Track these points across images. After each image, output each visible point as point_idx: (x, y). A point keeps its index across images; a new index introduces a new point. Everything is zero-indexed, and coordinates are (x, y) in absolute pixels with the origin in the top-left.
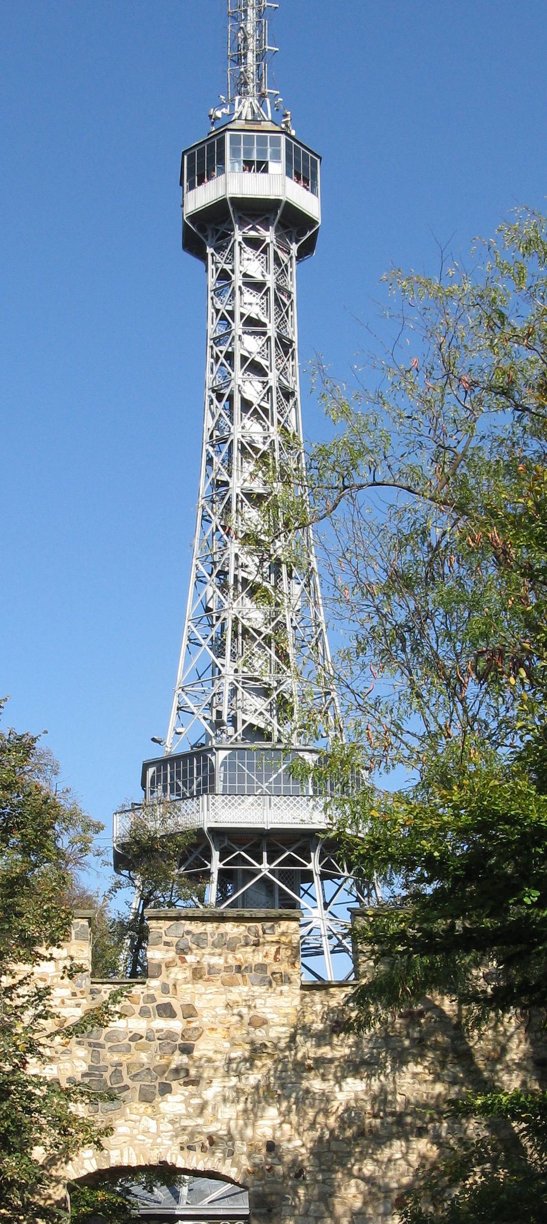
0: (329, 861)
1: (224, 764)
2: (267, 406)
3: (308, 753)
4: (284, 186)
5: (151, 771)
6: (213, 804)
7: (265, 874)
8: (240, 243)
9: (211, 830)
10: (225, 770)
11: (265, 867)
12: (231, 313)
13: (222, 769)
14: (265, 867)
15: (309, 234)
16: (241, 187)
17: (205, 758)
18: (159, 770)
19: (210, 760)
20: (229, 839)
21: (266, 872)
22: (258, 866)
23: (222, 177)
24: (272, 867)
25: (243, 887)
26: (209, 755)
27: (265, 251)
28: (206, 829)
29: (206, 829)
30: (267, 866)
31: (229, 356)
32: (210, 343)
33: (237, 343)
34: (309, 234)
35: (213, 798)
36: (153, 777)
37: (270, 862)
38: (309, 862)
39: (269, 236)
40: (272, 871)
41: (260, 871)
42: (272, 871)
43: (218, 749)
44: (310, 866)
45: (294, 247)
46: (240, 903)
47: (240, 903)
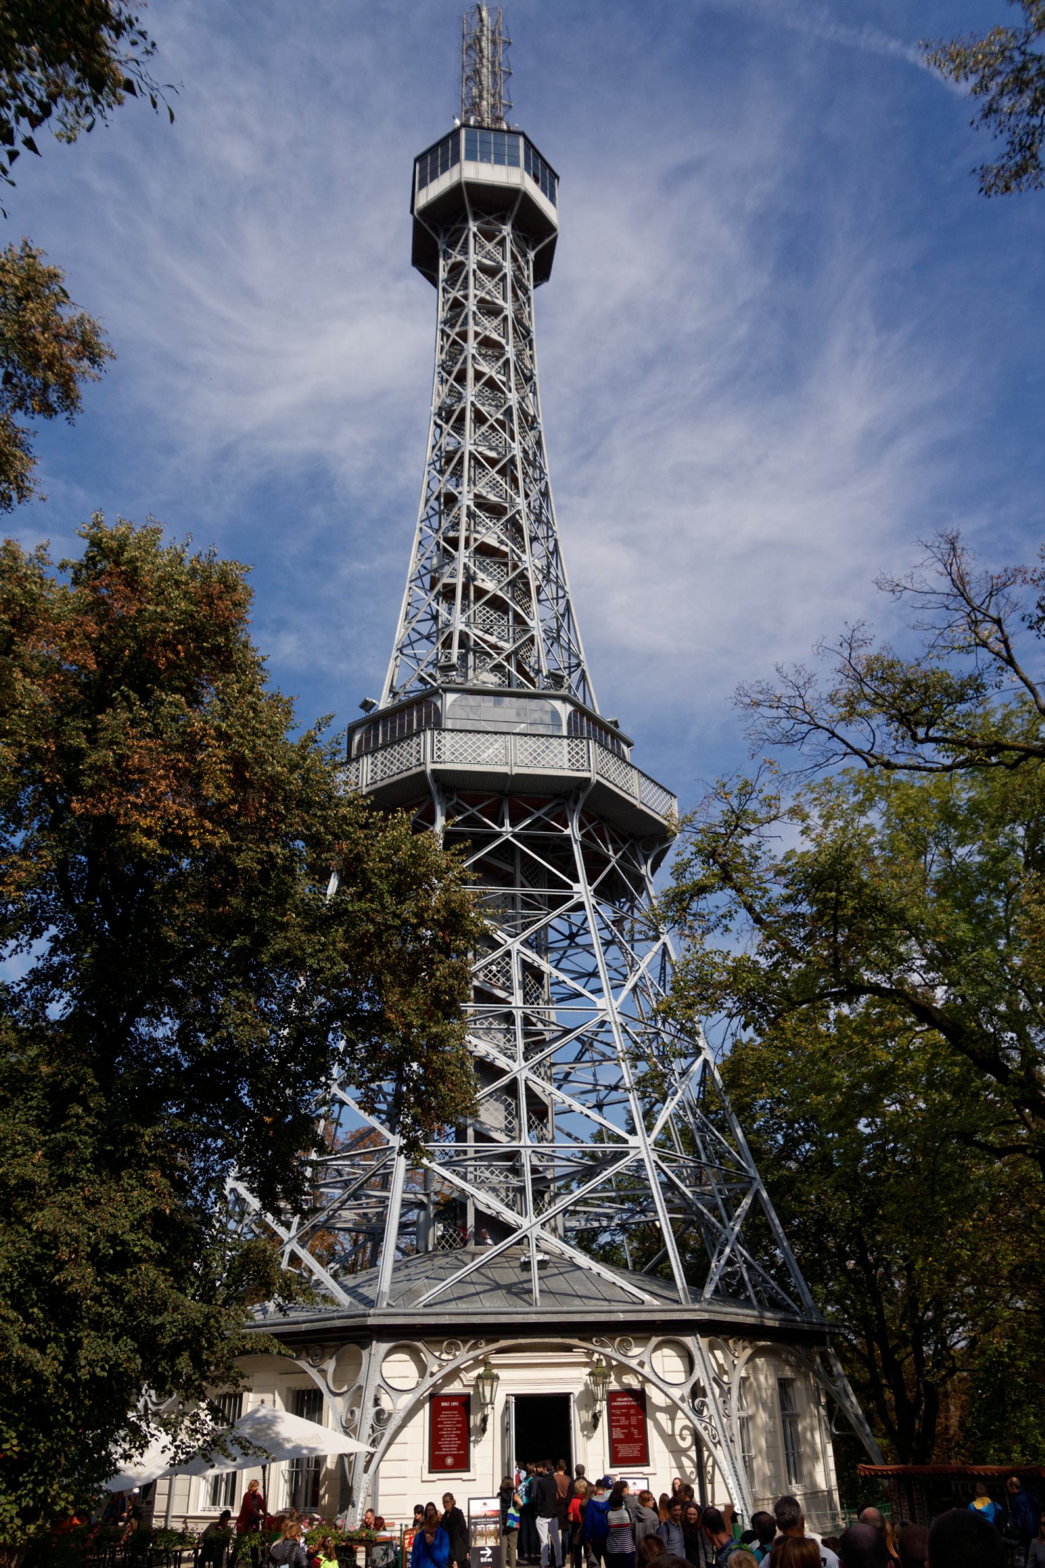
0: (588, 832)
2: (504, 379)
4: (523, 178)
7: (507, 841)
8: (475, 235)
9: (433, 771)
11: (507, 830)
12: (466, 297)
14: (507, 830)
15: (547, 240)
16: (477, 172)
18: (368, 732)
20: (459, 797)
22: (498, 829)
23: (457, 167)
27: (502, 243)
28: (428, 771)
29: (428, 771)
30: (510, 829)
31: (463, 335)
34: (547, 240)
36: (360, 742)
37: (513, 825)
38: (566, 827)
39: (507, 229)
40: (515, 836)
41: (499, 835)
43: (445, 691)
44: (567, 832)
45: (531, 255)
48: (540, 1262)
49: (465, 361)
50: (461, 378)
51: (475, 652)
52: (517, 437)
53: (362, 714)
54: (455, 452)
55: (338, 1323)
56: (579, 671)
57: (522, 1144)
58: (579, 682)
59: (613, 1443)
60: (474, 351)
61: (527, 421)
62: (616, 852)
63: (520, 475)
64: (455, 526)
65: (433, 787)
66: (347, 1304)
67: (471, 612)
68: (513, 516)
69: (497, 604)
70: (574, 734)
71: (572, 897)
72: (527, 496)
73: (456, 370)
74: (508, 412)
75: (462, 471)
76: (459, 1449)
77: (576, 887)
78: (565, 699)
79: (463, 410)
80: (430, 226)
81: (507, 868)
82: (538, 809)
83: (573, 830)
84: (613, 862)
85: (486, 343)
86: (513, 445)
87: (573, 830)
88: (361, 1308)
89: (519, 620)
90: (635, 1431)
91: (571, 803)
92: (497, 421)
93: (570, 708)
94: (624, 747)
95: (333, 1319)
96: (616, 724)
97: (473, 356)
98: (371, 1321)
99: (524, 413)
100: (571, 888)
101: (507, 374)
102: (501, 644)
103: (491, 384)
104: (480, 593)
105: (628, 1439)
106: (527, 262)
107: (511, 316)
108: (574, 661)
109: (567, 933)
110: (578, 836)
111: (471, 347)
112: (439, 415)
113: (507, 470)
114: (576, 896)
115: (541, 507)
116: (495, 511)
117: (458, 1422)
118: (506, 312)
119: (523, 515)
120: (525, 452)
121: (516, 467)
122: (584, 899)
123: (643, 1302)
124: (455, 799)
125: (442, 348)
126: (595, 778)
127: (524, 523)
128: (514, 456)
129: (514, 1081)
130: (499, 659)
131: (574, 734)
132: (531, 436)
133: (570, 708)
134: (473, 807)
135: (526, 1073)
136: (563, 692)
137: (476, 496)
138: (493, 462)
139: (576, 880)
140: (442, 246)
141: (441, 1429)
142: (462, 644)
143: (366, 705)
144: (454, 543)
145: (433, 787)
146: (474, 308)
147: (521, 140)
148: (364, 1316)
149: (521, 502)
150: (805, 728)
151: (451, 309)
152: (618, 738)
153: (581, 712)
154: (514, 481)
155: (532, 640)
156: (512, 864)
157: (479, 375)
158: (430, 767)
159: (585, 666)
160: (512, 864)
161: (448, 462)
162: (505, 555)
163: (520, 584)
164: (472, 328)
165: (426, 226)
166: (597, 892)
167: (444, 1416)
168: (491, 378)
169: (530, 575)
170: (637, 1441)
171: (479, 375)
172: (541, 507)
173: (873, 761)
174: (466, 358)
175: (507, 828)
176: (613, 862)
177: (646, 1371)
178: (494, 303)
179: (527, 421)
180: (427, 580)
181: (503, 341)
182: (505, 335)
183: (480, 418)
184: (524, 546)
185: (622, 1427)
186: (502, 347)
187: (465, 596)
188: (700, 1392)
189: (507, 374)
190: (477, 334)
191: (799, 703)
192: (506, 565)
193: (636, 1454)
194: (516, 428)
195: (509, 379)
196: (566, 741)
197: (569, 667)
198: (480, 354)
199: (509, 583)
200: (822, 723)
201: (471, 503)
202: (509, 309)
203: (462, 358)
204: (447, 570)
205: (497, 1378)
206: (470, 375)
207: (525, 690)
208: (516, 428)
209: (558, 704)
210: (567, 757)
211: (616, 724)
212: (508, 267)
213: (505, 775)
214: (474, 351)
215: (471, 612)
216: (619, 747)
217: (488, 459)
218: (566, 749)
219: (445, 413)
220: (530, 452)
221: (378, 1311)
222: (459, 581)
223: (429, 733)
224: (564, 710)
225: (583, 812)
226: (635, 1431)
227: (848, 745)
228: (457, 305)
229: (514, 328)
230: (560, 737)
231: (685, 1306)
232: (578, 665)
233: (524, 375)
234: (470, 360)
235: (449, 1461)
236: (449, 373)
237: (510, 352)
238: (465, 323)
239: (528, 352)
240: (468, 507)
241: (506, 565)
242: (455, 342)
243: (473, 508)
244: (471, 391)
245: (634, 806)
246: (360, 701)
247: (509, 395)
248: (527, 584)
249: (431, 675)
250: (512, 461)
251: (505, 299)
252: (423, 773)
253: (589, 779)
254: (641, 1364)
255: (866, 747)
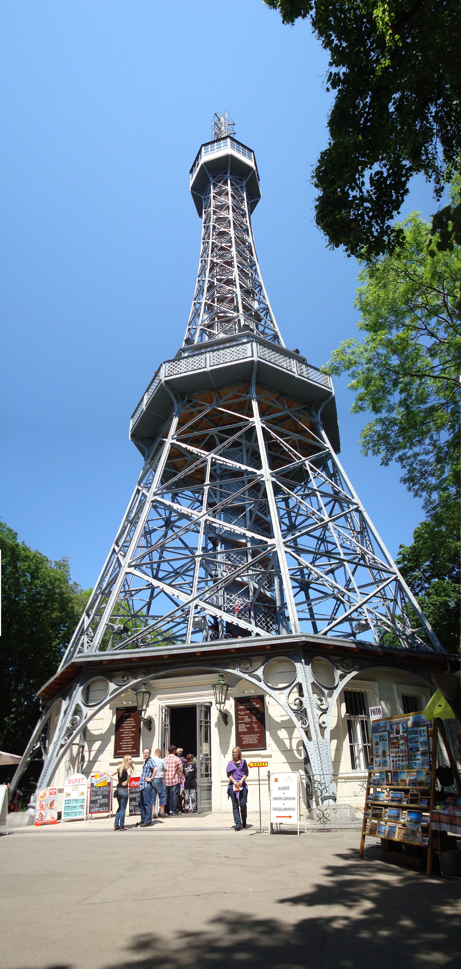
9: (166, 382)
45: (244, 183)
59: (239, 735)
80: (197, 192)
90: (255, 726)
105: (250, 731)
106: (242, 187)
117: (133, 727)
140: (203, 197)
141: (122, 733)
147: (229, 140)
165: (196, 193)
170: (256, 733)
185: (246, 723)
193: (256, 742)
212: (229, 188)
213: (205, 372)
226: (255, 726)
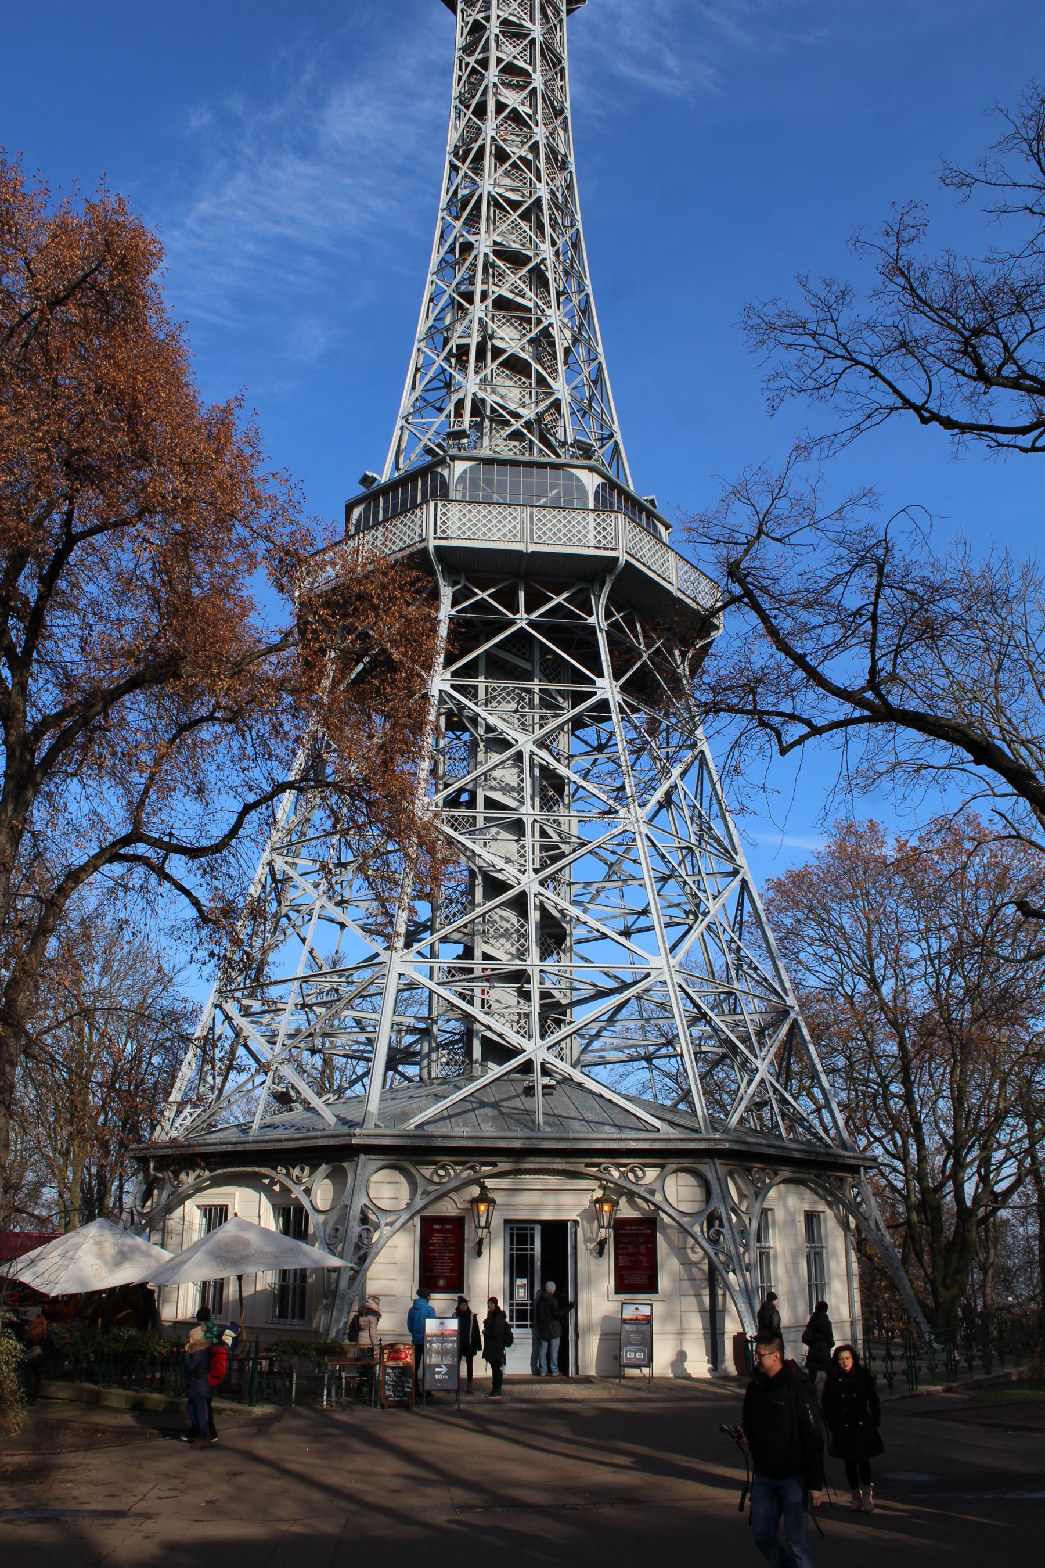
1: (462, 478)
2: (530, 112)
3: (586, 471)
5: (356, 512)
6: (444, 523)
7: (522, 628)
9: (437, 548)
10: (464, 488)
11: (522, 614)
13: (460, 487)
17: (435, 475)
18: (367, 510)
19: (442, 476)
20: (467, 580)
21: (523, 624)
22: (511, 616)
24: (533, 616)
25: (488, 640)
26: (439, 470)
28: (431, 549)
30: (525, 616)
31: (484, 63)
32: (458, 54)
33: (493, 45)
35: (444, 505)
36: (359, 521)
37: (529, 610)
38: (590, 614)
40: (531, 624)
42: (531, 624)
43: (453, 458)
44: (592, 620)
46: (482, 667)
47: (482, 667)
48: (544, 1087)
49: (485, 93)
50: (480, 111)
51: (491, 421)
52: (544, 176)
53: (362, 490)
54: (472, 195)
55: (321, 1142)
56: (612, 442)
57: (529, 962)
58: (613, 456)
60: (495, 80)
61: (556, 160)
62: (648, 647)
63: (546, 220)
64: (471, 279)
65: (438, 568)
66: (333, 1124)
67: (488, 371)
68: (538, 265)
69: (516, 366)
70: (603, 503)
71: (595, 693)
72: (554, 243)
73: (474, 102)
74: (535, 148)
75: (479, 217)
76: (452, 1270)
77: (599, 682)
78: (591, 469)
79: (482, 148)
81: (526, 666)
82: (557, 595)
83: (598, 620)
84: (645, 657)
85: (509, 69)
86: (539, 185)
87: (598, 620)
88: (345, 1130)
89: (542, 382)
91: (596, 587)
92: (521, 158)
93: (599, 480)
94: (661, 528)
95: (317, 1138)
96: (652, 502)
97: (495, 85)
98: (355, 1141)
99: (553, 151)
100: (594, 683)
101: (533, 105)
102: (521, 411)
103: (515, 117)
104: (497, 352)
107: (539, 39)
108: (607, 433)
109: (595, 744)
110: (604, 625)
111: (493, 75)
112: (456, 154)
113: (532, 213)
114: (599, 692)
115: (572, 261)
116: (516, 259)
118: (533, 35)
119: (549, 263)
120: (552, 192)
121: (541, 210)
122: (608, 695)
123: (658, 1130)
124: (463, 582)
125: (460, 78)
126: (624, 558)
127: (550, 274)
128: (539, 199)
129: (523, 895)
130: (516, 425)
131: (603, 503)
132: (560, 179)
133: (599, 480)
134: (483, 591)
135: (536, 888)
136: (591, 463)
137: (495, 243)
138: (515, 205)
139: (601, 675)
142: (476, 411)
143: (366, 481)
144: (469, 297)
145: (438, 568)
146: (497, 31)
148: (349, 1135)
149: (547, 251)
150: (839, 365)
151: (469, 33)
152: (650, 515)
153: (610, 485)
154: (540, 227)
155: (557, 405)
156: (531, 661)
157: (500, 107)
158: (432, 543)
159: (618, 437)
160: (531, 661)
161: (463, 208)
162: (529, 310)
163: (543, 341)
164: (493, 54)
166: (623, 688)
167: (436, 1238)
168: (515, 111)
169: (555, 332)
171: (500, 107)
172: (572, 261)
173: (927, 415)
174: (486, 87)
175: (522, 614)
176: (645, 657)
177: (658, 1198)
178: (522, 26)
179: (556, 160)
180: (439, 340)
181: (530, 69)
182: (532, 62)
183: (501, 156)
184: (549, 302)
186: (530, 76)
187: (481, 356)
188: (717, 1222)
189: (533, 105)
190: (499, 61)
191: (830, 329)
192: (529, 321)
194: (542, 166)
195: (536, 112)
196: (592, 516)
197: (602, 439)
198: (503, 84)
199: (531, 341)
200: (861, 358)
201: (489, 251)
202: (537, 31)
203: (481, 89)
204: (460, 328)
205: (492, 1202)
206: (491, 107)
207: (546, 460)
208: (542, 166)
209: (583, 475)
210: (593, 533)
211: (652, 502)
213: (520, 552)
214: (495, 80)
215: (488, 371)
216: (655, 528)
217: (509, 202)
218: (592, 524)
219: (461, 153)
220: (559, 195)
221: (363, 1131)
222: (474, 341)
223: (432, 504)
224: (591, 482)
225: (610, 598)
226: (644, 1259)
227: (896, 391)
228: (477, 29)
229: (543, 54)
230: (584, 510)
231: (704, 1134)
232: (611, 436)
233: (554, 108)
234: (490, 90)
235: (441, 1282)
236: (467, 107)
237: (538, 81)
238: (486, 49)
239: (560, 83)
240: (486, 255)
241: (529, 321)
242: (474, 71)
243: (492, 257)
244: (491, 126)
245: (670, 593)
246: (360, 476)
247: (535, 129)
248: (552, 345)
249: (439, 446)
250: (538, 202)
251: (532, 20)
252: (425, 550)
253: (617, 559)
254: (652, 1192)
255: (919, 400)
